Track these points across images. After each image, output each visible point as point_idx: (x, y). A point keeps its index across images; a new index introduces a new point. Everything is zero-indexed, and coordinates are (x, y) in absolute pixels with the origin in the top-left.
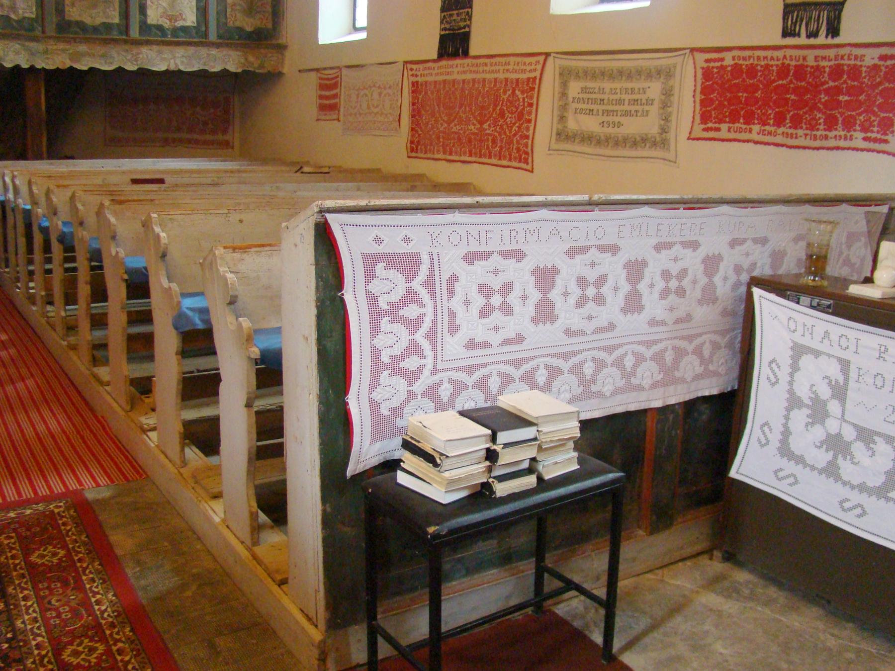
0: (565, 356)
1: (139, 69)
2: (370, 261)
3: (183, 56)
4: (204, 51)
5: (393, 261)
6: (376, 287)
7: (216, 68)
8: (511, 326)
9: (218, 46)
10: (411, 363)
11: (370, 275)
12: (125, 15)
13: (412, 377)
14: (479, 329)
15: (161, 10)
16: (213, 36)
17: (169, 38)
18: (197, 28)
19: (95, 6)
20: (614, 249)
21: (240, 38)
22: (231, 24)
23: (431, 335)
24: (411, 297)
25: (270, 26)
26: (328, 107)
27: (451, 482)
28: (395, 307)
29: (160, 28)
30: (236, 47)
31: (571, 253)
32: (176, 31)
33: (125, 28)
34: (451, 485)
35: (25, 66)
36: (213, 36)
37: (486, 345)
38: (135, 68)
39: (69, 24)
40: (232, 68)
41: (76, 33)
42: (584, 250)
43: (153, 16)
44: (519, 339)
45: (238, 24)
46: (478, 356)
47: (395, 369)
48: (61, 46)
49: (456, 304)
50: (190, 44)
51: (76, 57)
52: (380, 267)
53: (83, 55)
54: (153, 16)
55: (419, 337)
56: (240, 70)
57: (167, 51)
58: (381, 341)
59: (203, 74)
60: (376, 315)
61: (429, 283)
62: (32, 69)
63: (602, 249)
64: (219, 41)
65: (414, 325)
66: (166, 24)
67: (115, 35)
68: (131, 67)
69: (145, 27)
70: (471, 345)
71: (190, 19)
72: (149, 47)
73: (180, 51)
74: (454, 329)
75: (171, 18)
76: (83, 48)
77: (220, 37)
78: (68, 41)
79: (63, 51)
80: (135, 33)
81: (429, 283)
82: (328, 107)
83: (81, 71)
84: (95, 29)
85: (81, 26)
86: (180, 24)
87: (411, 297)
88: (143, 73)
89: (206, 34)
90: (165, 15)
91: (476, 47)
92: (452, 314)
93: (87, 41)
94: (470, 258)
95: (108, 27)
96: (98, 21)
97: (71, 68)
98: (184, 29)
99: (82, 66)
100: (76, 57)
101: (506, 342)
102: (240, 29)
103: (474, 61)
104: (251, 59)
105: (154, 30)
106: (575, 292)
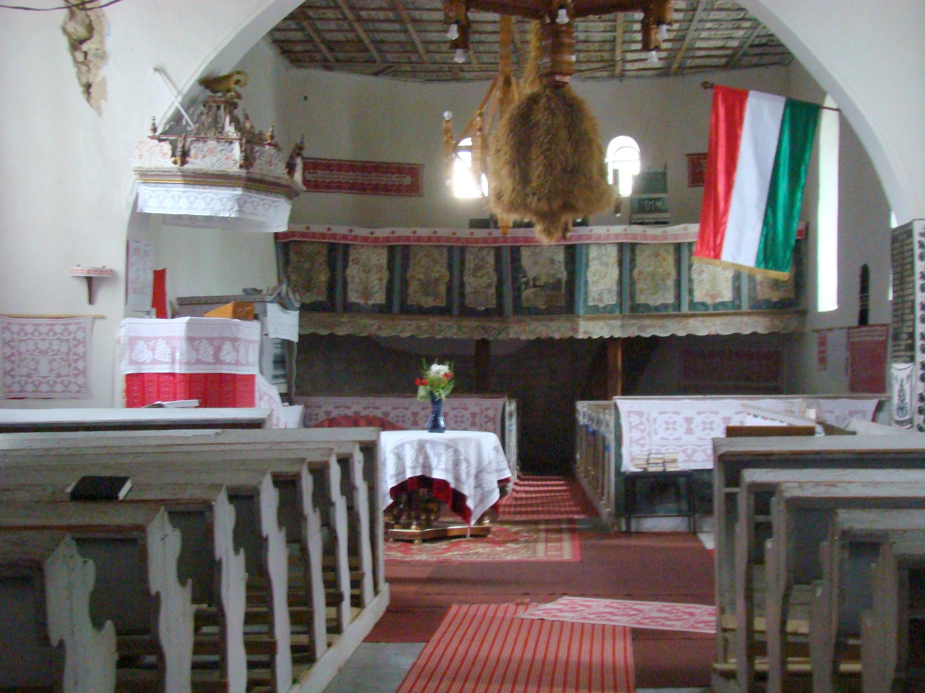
0: (700, 446)
1: (688, 335)
2: (629, 413)
3: (721, 324)
4: (737, 319)
5: (636, 413)
6: (631, 419)
7: (747, 331)
8: (677, 434)
9: (749, 314)
10: (642, 442)
11: (629, 417)
12: (678, 296)
13: (643, 446)
14: (666, 434)
15: (704, 292)
16: (745, 307)
17: (711, 311)
18: (733, 302)
19: (656, 293)
20: (716, 413)
21: (767, 307)
22: (759, 297)
23: (649, 434)
24: (641, 423)
25: (792, 296)
26: (822, 360)
27: (636, 465)
28: (636, 426)
29: (703, 304)
30: (764, 314)
31: (699, 413)
32: (715, 306)
33: (678, 306)
34: (636, 466)
35: (607, 336)
36: (745, 307)
37: (667, 439)
38: (684, 334)
39: (639, 306)
40: (761, 330)
41: (643, 312)
42: (704, 413)
43: (698, 296)
44: (680, 439)
45: (766, 297)
46: (664, 442)
47: (637, 442)
48: (633, 321)
49: (656, 426)
50: (726, 314)
51: (642, 328)
52: (632, 414)
53: (649, 326)
54: (698, 296)
55: (645, 434)
56: (767, 332)
57: (709, 321)
58: (633, 434)
59: (737, 336)
60: (631, 428)
61: (647, 419)
62: (612, 338)
63: (712, 412)
64: (751, 311)
65: (643, 431)
66: (709, 301)
67: (671, 311)
68: (681, 333)
69: (692, 305)
70: (662, 439)
71: (727, 295)
72: (695, 319)
73: (719, 321)
74: (656, 433)
75: (714, 297)
76: (647, 322)
77: (751, 307)
78: (638, 318)
79: (634, 325)
80: (685, 309)
81: (647, 419)
82: (822, 360)
83: (646, 339)
84: (656, 308)
85: (647, 307)
86: (719, 300)
87: (641, 423)
88: (691, 339)
89: (739, 307)
90: (706, 295)
91: (872, 319)
92: (655, 429)
93: (651, 317)
94: (662, 413)
95: (665, 306)
96: (659, 302)
97: (638, 337)
98: (723, 304)
99: (647, 334)
100: (642, 328)
101: (676, 439)
102: (768, 301)
103: (870, 328)
104: (777, 322)
105: (699, 306)
106: (701, 426)
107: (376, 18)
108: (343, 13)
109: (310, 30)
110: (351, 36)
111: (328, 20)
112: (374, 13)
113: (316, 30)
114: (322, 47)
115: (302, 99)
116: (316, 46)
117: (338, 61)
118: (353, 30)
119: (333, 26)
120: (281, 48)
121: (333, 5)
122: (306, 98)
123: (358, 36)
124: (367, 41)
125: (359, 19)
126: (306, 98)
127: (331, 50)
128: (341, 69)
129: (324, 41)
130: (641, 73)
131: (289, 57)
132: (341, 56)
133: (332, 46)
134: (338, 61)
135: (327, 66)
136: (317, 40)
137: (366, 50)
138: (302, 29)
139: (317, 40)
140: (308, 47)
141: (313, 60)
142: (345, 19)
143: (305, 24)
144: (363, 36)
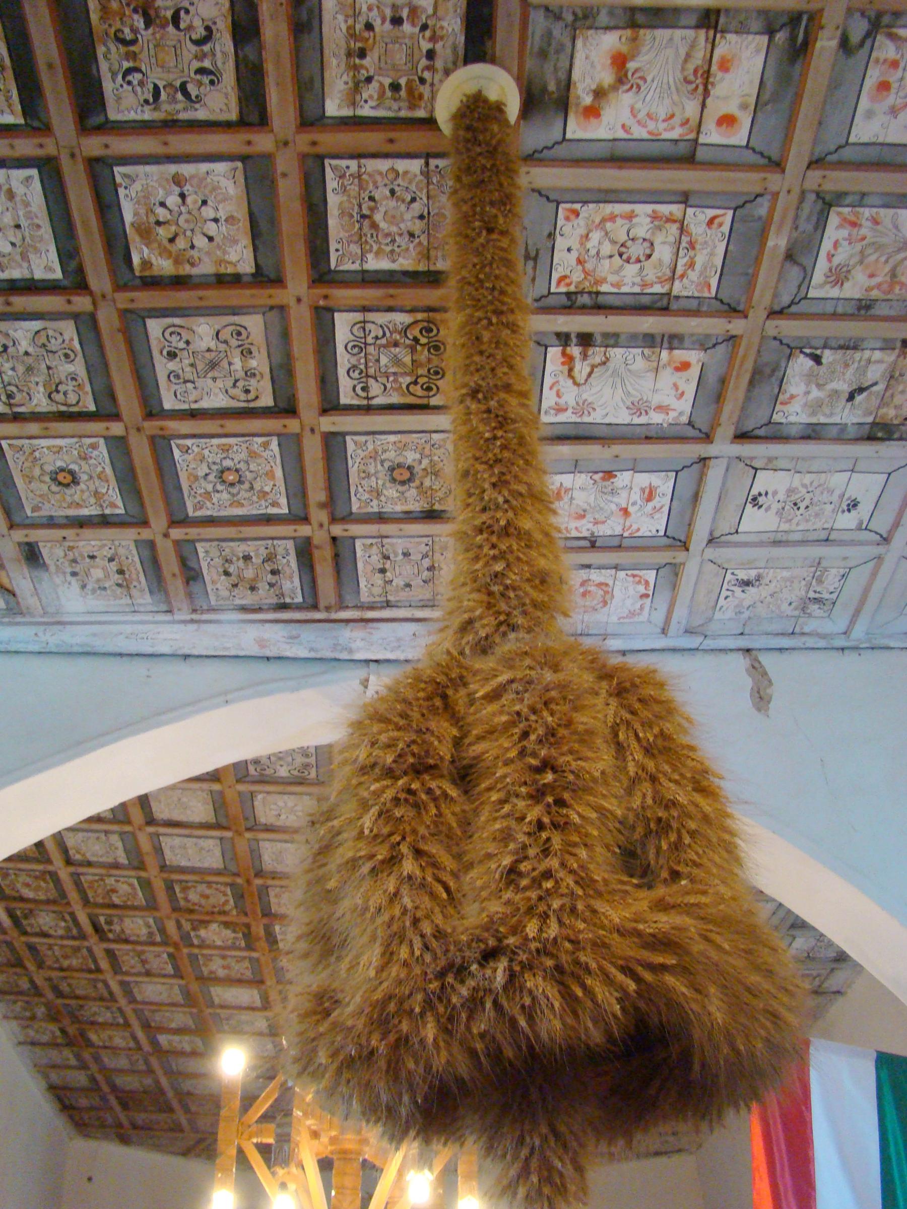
107: (179, 1047)
108: (134, 1038)
109: (94, 1068)
110: (148, 1081)
111: (114, 1049)
112: (176, 1038)
113: (103, 1069)
114: (113, 1101)
115: (85, 1179)
116: (103, 1098)
117: (135, 1127)
118: (150, 1071)
119: (123, 1063)
120: (60, 1099)
121: (121, 1021)
122: (90, 1179)
123: (157, 1082)
124: (170, 1094)
125: (154, 1043)
126: (90, 1179)
127: (125, 1106)
128: (140, 1144)
129: (114, 1088)
130: (785, 642)
131: (71, 1117)
132: (141, 1118)
133: (127, 1100)
134: (135, 1127)
135: (125, 1140)
136: (105, 1088)
137: (171, 1110)
138: (84, 1066)
139: (105, 1088)
140: (96, 1101)
141: (103, 1126)
142: (139, 1048)
143: (86, 1055)
144: (164, 1082)
